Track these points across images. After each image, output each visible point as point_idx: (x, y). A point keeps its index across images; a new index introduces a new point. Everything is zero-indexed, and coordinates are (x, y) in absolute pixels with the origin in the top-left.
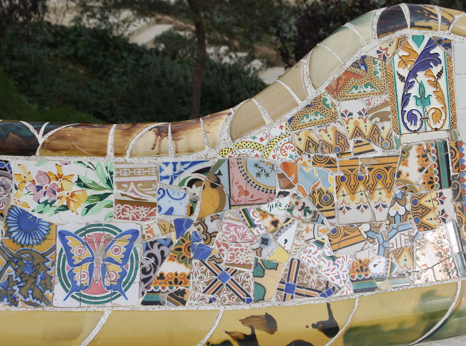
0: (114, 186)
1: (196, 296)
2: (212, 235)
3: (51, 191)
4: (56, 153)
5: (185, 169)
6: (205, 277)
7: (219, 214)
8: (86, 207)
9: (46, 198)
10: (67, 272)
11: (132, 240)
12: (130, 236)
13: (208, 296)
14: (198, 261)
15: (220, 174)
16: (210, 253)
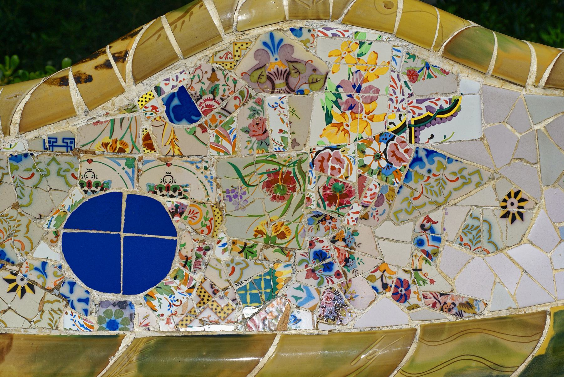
9: (345, 97)
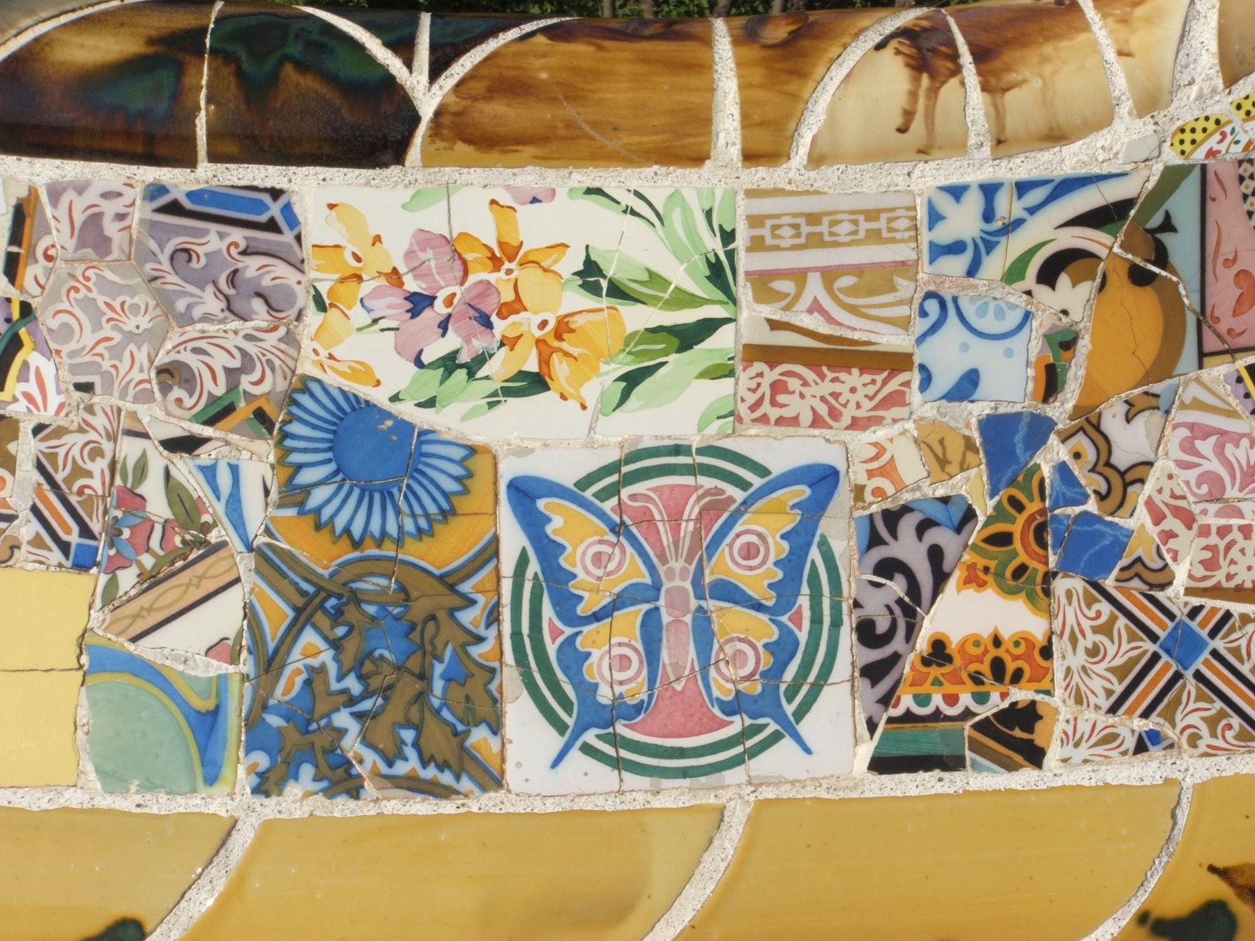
0: (744, 291)
1: (1084, 728)
2: (1129, 477)
3: (472, 313)
4: (495, 155)
5: (1032, 211)
6: (1112, 650)
7: (1156, 388)
8: (620, 379)
9: (452, 342)
10: (552, 649)
11: (814, 510)
12: (803, 492)
13: (1131, 725)
14: (1077, 584)
15: (1168, 225)
16: (1123, 547)
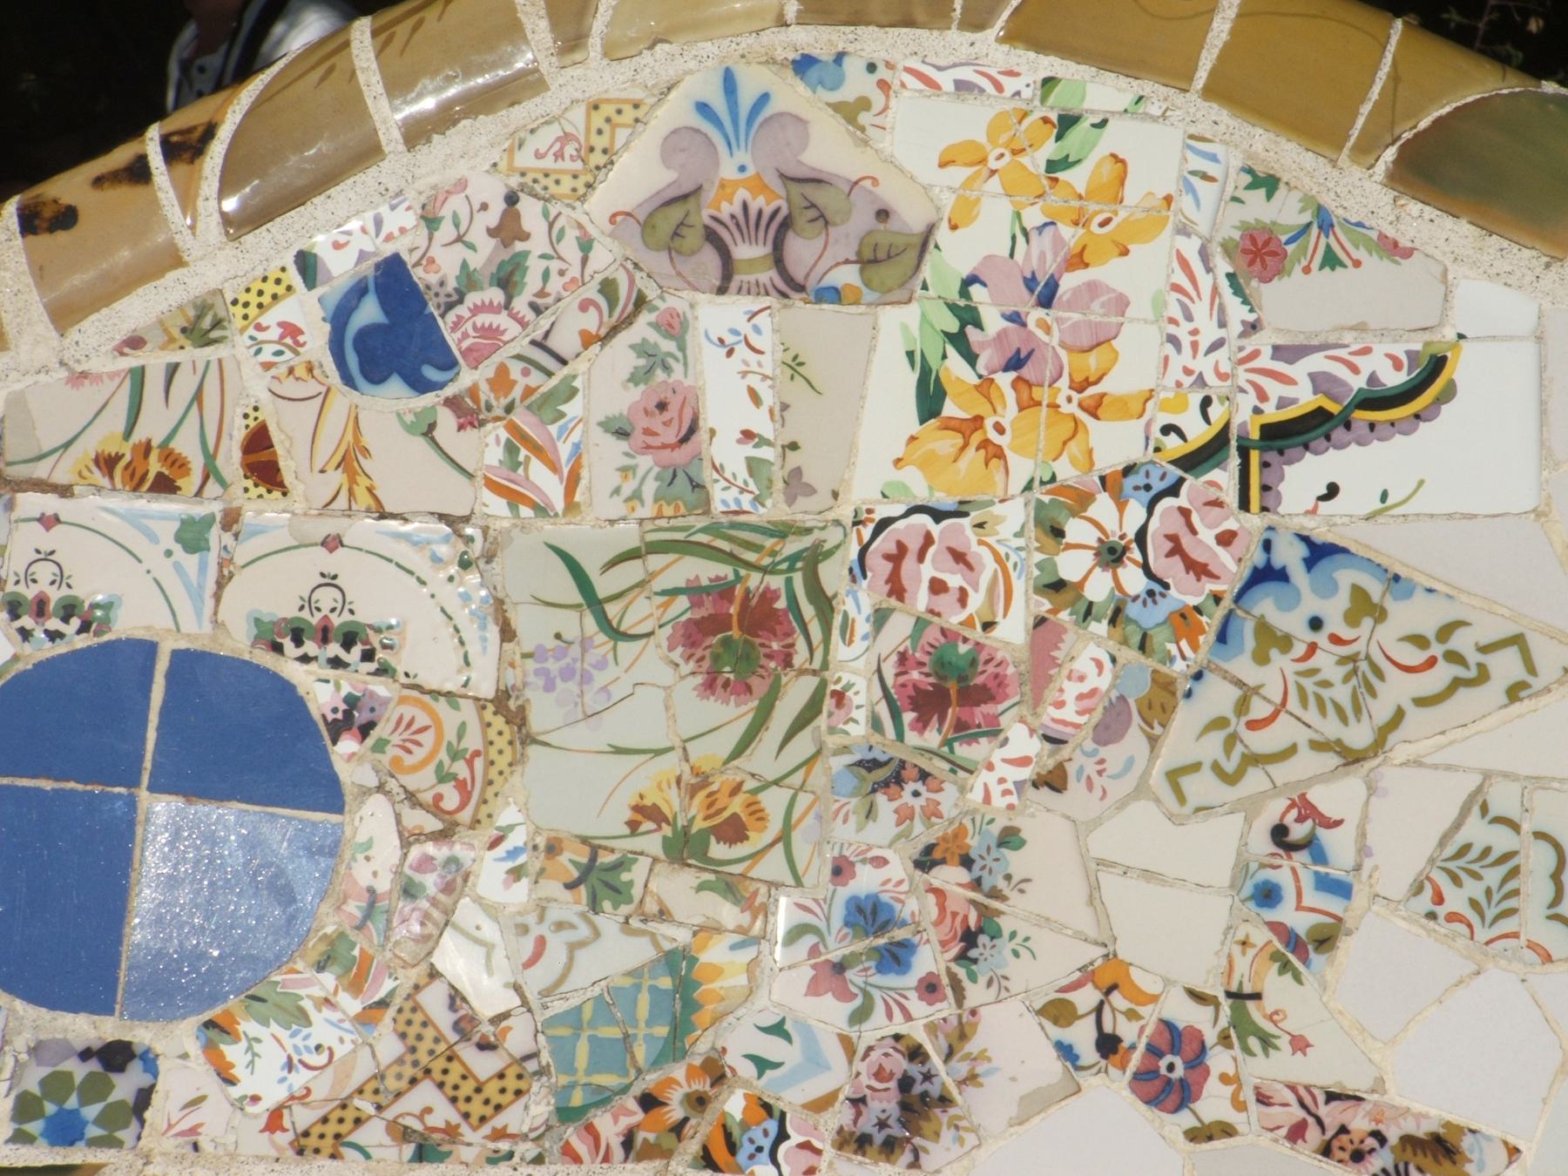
9: (993, 321)
